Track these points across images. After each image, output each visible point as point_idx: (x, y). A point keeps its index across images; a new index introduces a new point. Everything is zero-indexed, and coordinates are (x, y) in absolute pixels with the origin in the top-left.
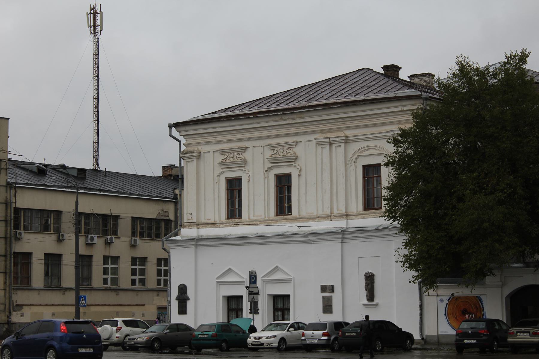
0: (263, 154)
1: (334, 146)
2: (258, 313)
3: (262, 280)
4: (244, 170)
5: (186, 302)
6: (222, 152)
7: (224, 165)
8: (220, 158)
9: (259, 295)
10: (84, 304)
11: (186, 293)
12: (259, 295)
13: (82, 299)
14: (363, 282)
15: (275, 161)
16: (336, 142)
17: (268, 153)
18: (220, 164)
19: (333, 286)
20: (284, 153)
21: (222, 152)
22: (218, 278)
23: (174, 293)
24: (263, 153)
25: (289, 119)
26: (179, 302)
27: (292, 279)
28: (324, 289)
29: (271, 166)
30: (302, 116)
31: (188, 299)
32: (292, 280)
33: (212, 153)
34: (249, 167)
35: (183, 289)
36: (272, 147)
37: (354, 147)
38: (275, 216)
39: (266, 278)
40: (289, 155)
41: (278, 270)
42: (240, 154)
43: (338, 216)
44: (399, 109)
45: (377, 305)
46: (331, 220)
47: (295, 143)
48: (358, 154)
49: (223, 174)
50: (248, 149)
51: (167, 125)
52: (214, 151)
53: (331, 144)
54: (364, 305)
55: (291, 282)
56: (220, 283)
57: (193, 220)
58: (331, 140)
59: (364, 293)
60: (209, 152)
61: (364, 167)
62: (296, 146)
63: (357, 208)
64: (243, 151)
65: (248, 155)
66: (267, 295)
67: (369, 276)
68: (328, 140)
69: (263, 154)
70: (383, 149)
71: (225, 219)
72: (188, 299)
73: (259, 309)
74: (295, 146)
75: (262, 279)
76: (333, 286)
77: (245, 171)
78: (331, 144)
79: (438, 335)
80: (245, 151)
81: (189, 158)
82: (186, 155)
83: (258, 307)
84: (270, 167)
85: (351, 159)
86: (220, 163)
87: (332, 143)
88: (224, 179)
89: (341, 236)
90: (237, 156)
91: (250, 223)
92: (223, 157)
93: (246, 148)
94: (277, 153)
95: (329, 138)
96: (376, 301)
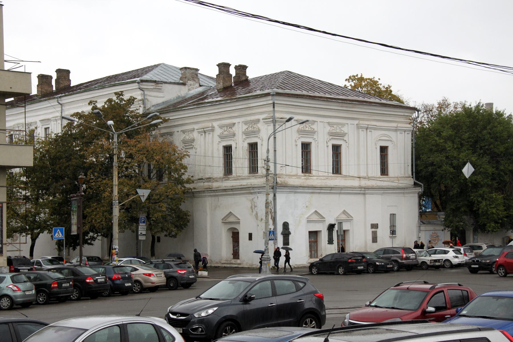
1: (368, 130)
2: (333, 243)
8: (328, 128)
10: (272, 238)
11: (289, 229)
17: (328, 128)
23: (280, 229)
25: (346, 107)
30: (355, 106)
35: (286, 225)
37: (377, 134)
40: (342, 132)
44: (402, 114)
53: (367, 129)
56: (309, 221)
58: (369, 126)
78: (367, 129)
95: (368, 125)
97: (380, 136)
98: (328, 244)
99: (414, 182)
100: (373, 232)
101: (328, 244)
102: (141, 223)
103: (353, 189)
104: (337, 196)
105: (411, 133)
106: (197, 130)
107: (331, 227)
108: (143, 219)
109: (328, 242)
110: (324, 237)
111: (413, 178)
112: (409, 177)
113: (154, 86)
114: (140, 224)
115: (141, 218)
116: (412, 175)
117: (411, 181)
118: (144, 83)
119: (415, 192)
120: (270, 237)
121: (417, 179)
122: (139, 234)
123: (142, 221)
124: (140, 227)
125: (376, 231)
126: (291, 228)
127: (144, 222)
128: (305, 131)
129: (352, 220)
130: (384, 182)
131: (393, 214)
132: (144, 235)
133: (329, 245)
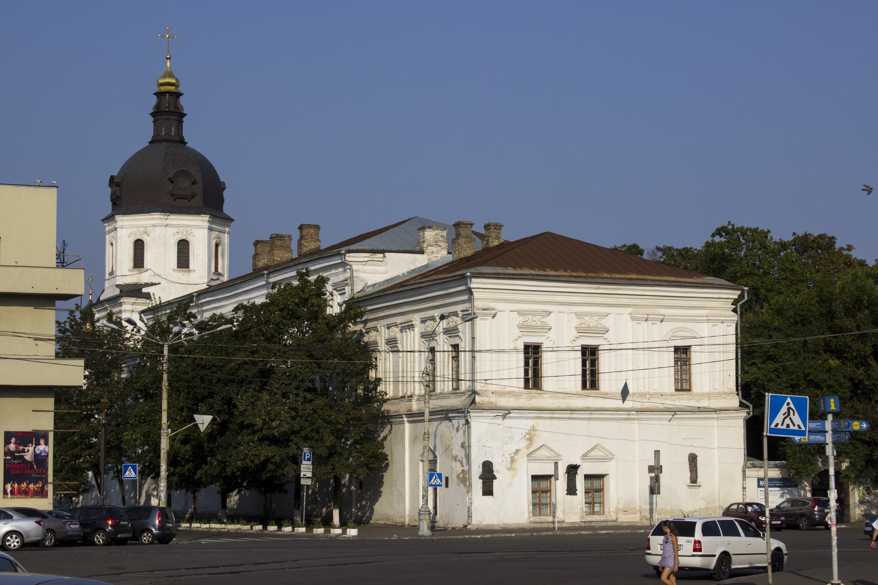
2: (576, 494)
6: (521, 313)
7: (524, 328)
10: (437, 484)
11: (492, 471)
13: (434, 477)
15: (582, 331)
16: (653, 319)
17: (575, 322)
18: (520, 327)
21: (521, 313)
23: (477, 470)
26: (484, 483)
36: (579, 315)
40: (600, 326)
44: (717, 296)
45: (700, 486)
54: (689, 486)
59: (688, 474)
65: (550, 320)
68: (646, 316)
70: (696, 332)
81: (485, 315)
82: (482, 312)
90: (541, 320)
92: (521, 318)
95: (648, 315)
97: (673, 331)
98: (567, 494)
99: (741, 402)
101: (567, 494)
102: (304, 460)
103: (612, 412)
104: (586, 422)
105: (734, 325)
106: (400, 324)
107: (572, 470)
108: (308, 455)
109: (566, 492)
110: (560, 485)
111: (738, 394)
112: (731, 393)
113: (369, 257)
114: (304, 462)
115: (305, 453)
116: (737, 390)
117: (735, 401)
118: (351, 254)
119: (740, 417)
120: (432, 481)
121: (744, 397)
122: (302, 476)
123: (306, 457)
124: (302, 466)
127: (309, 460)
128: (529, 327)
129: (611, 459)
130: (683, 401)
131: (658, 451)
132: (308, 478)
133: (568, 496)
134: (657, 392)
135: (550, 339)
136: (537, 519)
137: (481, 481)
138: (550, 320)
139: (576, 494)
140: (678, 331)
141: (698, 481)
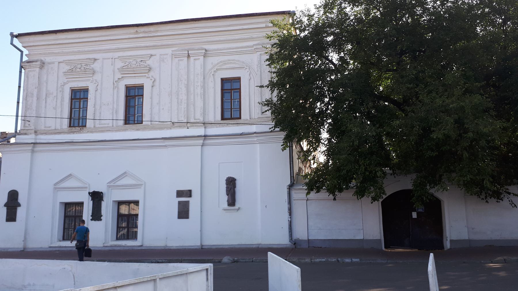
0: (113, 66)
1: (192, 59)
2: (101, 220)
3: (108, 186)
4: (91, 80)
5: (16, 209)
9: (103, 201)
12: (103, 201)
14: (224, 186)
17: (119, 64)
19: (190, 191)
20: (136, 65)
22: (55, 184)
24: (113, 64)
26: (7, 209)
27: (142, 184)
28: (180, 194)
29: (122, 77)
31: (19, 205)
32: (142, 186)
33: (56, 64)
34: (97, 77)
37: (212, 61)
38: (123, 125)
39: (112, 184)
41: (126, 176)
42: (89, 65)
43: (195, 124)
46: (188, 128)
47: (150, 56)
48: (216, 68)
49: (67, 84)
50: (98, 61)
51: (9, 33)
52: (59, 63)
54: (225, 210)
55: (141, 188)
57: (31, 127)
59: (225, 198)
60: (53, 63)
61: (222, 80)
62: (150, 59)
63: (215, 117)
64: (92, 63)
65: (96, 66)
66: (112, 201)
67: (231, 181)
69: (113, 66)
71: (68, 127)
72: (19, 205)
73: (102, 216)
74: (149, 59)
75: (108, 185)
76: (190, 191)
77: (92, 82)
79: (309, 240)
80: (93, 63)
83: (101, 213)
84: (121, 77)
85: (210, 72)
86: (65, 72)
87: (190, 56)
88: (69, 89)
89: (202, 141)
91: (95, 130)
93: (95, 60)
94: (129, 65)
96: (237, 206)
98: (92, 220)
100: (180, 203)
101: (92, 220)
109: (91, 218)
125: (187, 203)
126: (21, 199)
133: (93, 221)
134: (198, 121)
135: (95, 82)
136: (449, 240)
137: (6, 208)
138: (96, 66)
139: (101, 220)
140: (225, 64)
141: (237, 203)
